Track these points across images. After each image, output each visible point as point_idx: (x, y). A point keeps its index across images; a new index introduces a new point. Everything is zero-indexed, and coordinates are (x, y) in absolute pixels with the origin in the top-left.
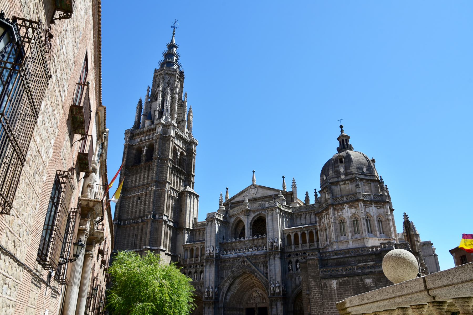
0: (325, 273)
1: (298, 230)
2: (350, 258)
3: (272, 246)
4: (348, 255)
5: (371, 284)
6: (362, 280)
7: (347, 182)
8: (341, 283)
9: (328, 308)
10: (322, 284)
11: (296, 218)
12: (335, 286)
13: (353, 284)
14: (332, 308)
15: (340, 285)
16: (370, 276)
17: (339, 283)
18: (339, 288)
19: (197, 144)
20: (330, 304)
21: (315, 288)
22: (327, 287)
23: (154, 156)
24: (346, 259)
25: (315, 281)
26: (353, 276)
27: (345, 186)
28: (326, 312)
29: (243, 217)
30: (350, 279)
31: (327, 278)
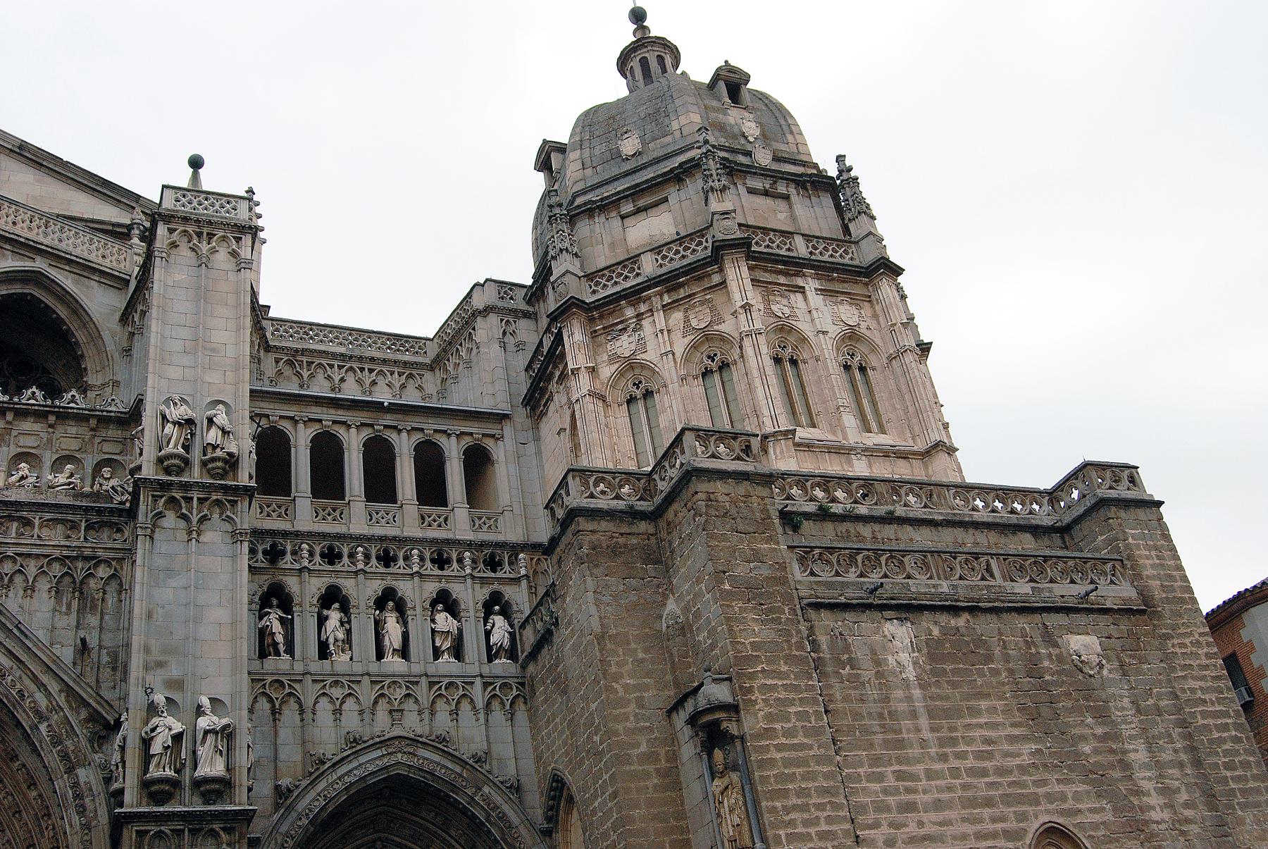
0: (826, 575)
1: (341, 415)
2: (909, 528)
5: (1101, 666)
6: (1049, 638)
7: (782, 188)
9: (881, 808)
10: (823, 640)
11: (280, 373)
12: (904, 657)
15: (932, 657)
16: (1081, 619)
18: (934, 672)
20: (891, 782)
21: (770, 661)
22: (852, 663)
25: (770, 615)
27: (769, 201)
30: (987, 626)
31: (846, 607)
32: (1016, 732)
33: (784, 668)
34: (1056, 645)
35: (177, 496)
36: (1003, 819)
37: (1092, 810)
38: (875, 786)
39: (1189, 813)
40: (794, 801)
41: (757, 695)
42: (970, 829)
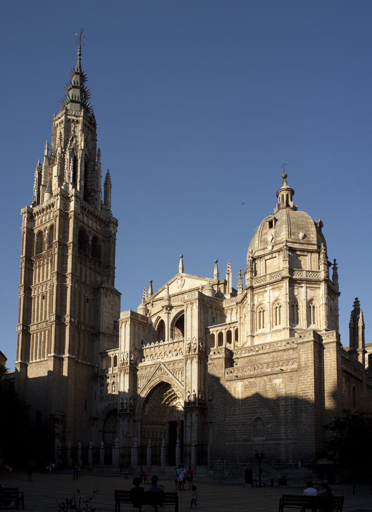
0: (231, 374)
3: (190, 348)
4: (261, 352)
6: (270, 381)
8: (247, 385)
9: (230, 415)
13: (260, 386)
14: (234, 415)
15: (245, 388)
17: (245, 385)
19: (117, 225)
21: (218, 392)
23: (54, 241)
24: (258, 357)
26: (261, 376)
28: (228, 419)
29: (163, 316)
30: (257, 380)
32: (257, 400)
33: (220, 393)
34: (271, 382)
35: (188, 357)
36: (250, 416)
37: (268, 415)
38: (229, 412)
39: (289, 414)
40: (217, 414)
41: (215, 398)
42: (243, 418)
